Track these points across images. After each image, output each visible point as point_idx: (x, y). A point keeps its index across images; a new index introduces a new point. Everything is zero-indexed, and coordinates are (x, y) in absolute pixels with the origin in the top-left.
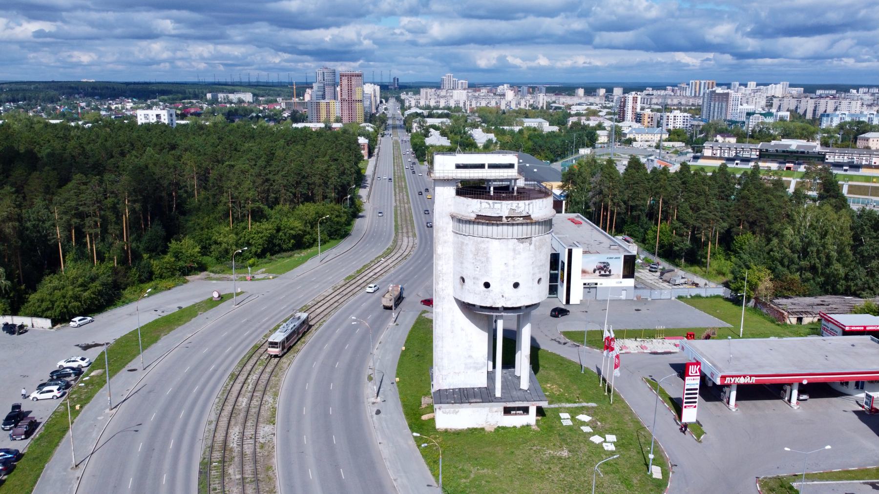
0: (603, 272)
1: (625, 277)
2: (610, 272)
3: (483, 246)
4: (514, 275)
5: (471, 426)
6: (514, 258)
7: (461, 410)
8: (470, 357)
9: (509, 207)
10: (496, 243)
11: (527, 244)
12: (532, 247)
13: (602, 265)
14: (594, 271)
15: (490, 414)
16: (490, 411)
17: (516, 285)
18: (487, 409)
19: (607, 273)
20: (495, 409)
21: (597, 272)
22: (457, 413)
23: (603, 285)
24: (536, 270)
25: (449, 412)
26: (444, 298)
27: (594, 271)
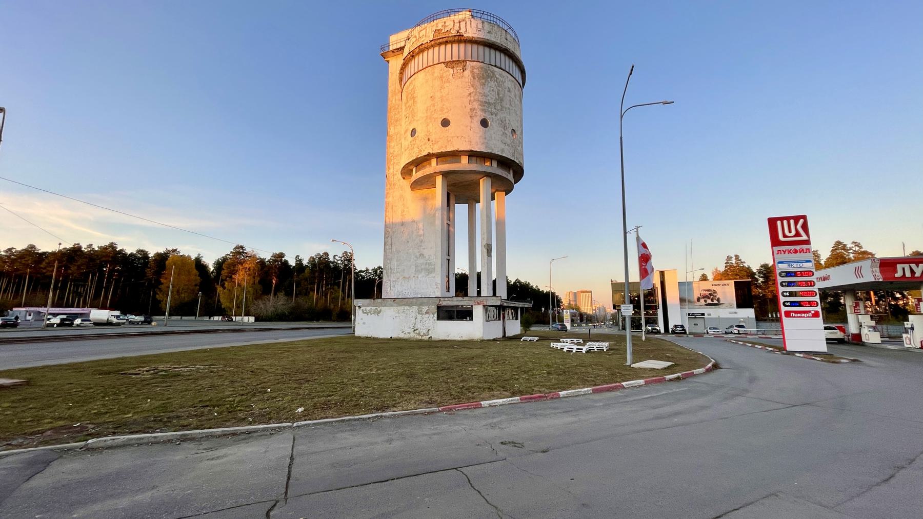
0: (709, 301)
1: (739, 306)
2: (718, 300)
3: (411, 87)
4: (442, 110)
5: (394, 336)
6: (442, 88)
7: (383, 309)
8: (422, 255)
9: (434, 29)
10: (421, 75)
11: (460, 69)
12: (467, 73)
13: (707, 293)
14: (698, 300)
15: (419, 316)
16: (420, 312)
17: (445, 123)
18: (415, 308)
19: (715, 302)
20: (425, 309)
21: (702, 301)
22: (379, 312)
23: (712, 316)
24: (476, 105)
25: (370, 312)
26: (394, 184)
27: (698, 300)
